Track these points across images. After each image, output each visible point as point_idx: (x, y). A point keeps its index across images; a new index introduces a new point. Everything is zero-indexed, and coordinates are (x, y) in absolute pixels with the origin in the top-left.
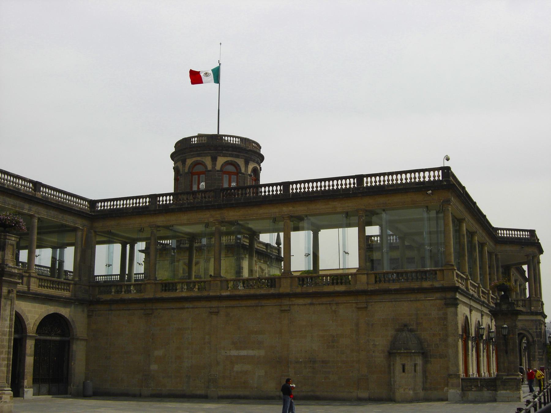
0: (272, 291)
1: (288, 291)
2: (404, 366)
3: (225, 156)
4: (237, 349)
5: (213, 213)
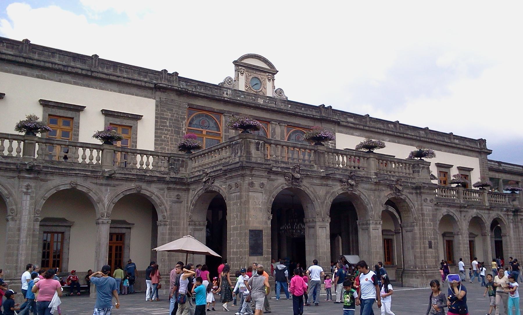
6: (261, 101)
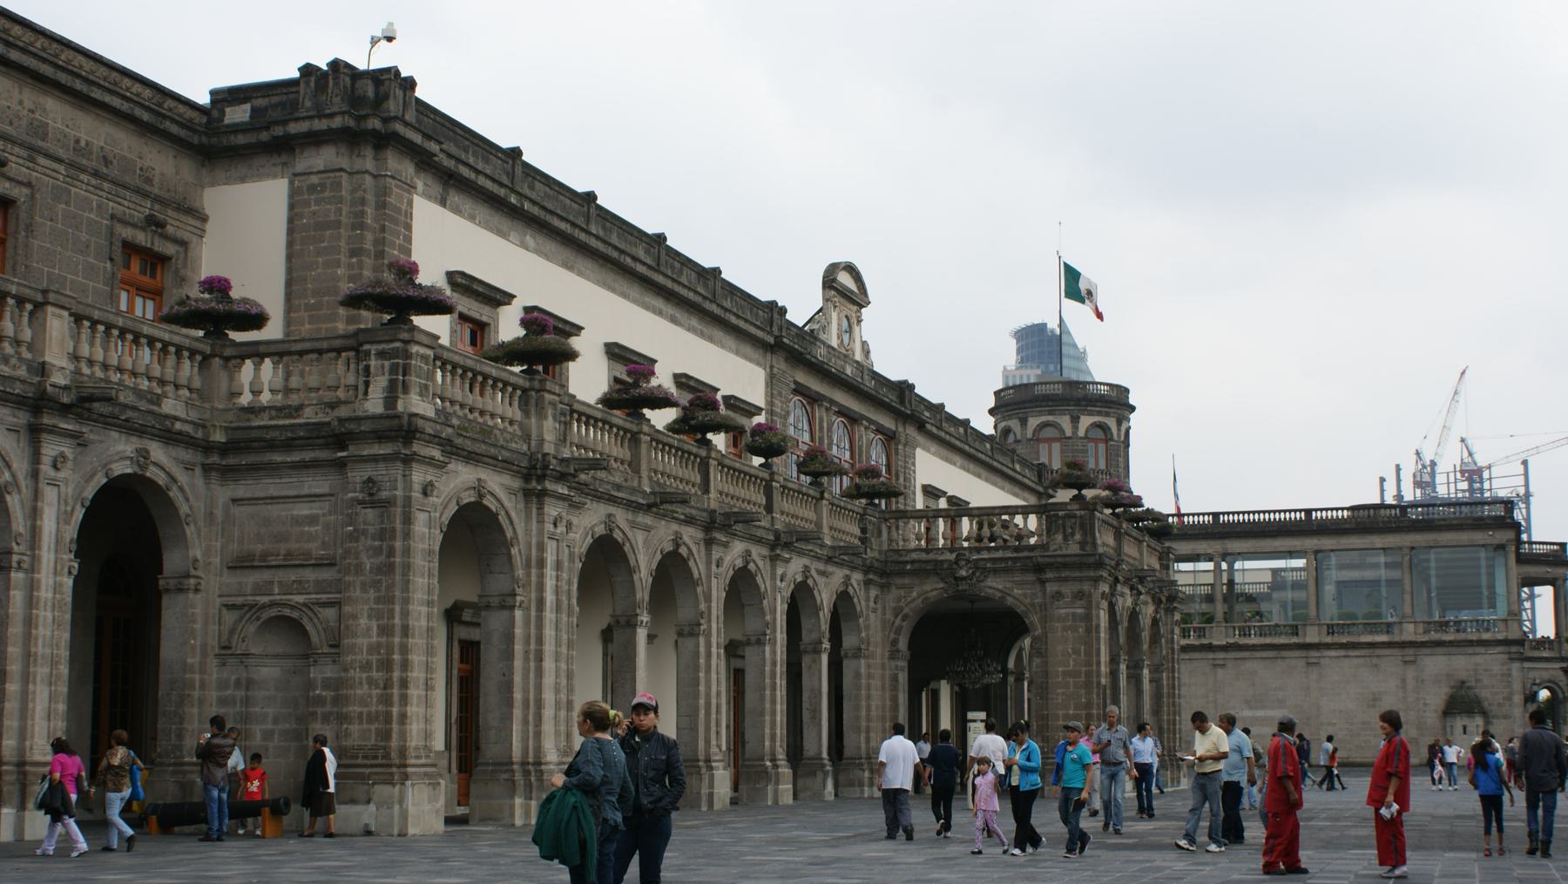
0: (1294, 640)
1: (1316, 640)
2: (1465, 728)
3: (1091, 414)
4: (1251, 708)
5: (1212, 543)
6: (849, 371)
